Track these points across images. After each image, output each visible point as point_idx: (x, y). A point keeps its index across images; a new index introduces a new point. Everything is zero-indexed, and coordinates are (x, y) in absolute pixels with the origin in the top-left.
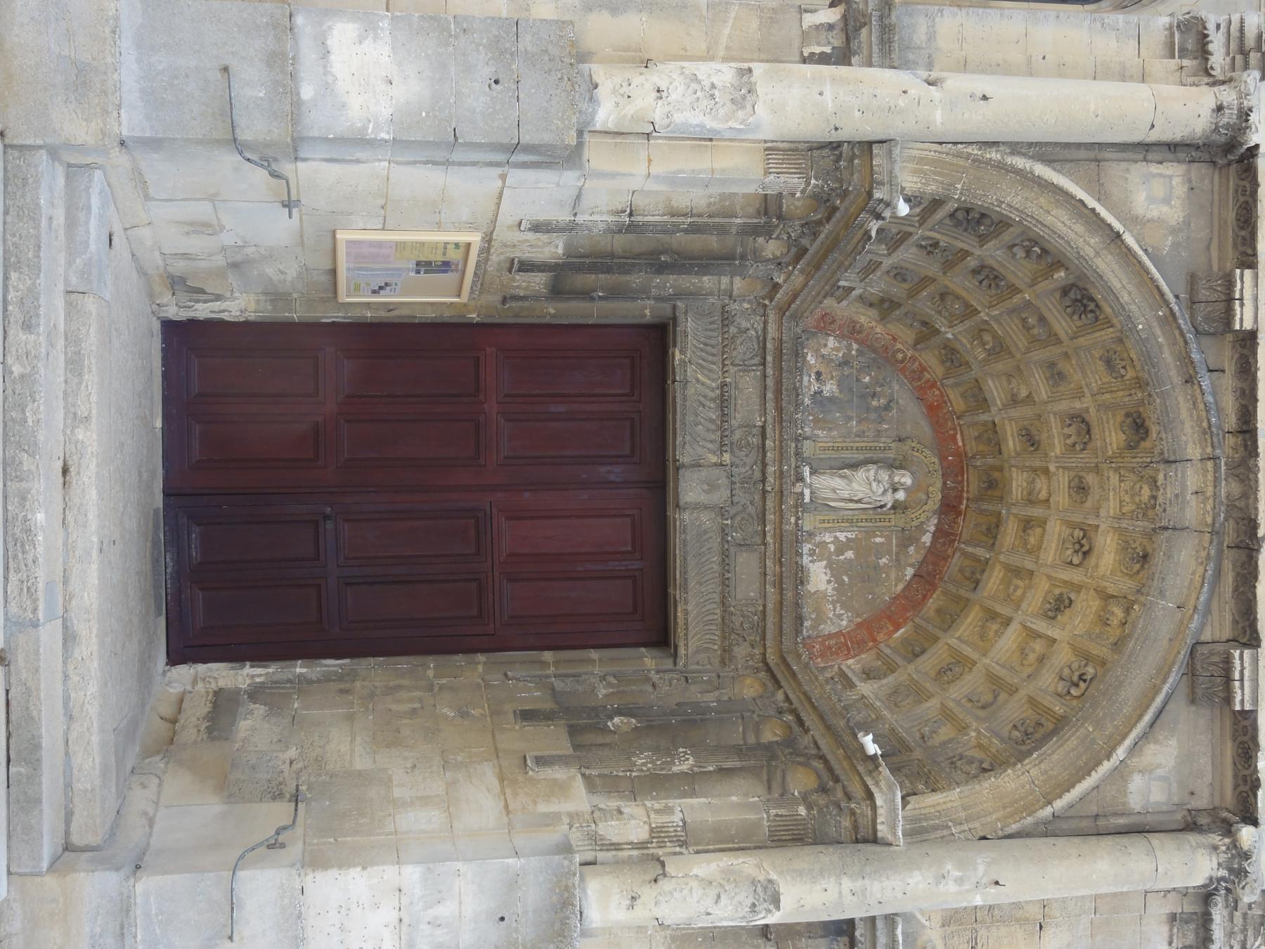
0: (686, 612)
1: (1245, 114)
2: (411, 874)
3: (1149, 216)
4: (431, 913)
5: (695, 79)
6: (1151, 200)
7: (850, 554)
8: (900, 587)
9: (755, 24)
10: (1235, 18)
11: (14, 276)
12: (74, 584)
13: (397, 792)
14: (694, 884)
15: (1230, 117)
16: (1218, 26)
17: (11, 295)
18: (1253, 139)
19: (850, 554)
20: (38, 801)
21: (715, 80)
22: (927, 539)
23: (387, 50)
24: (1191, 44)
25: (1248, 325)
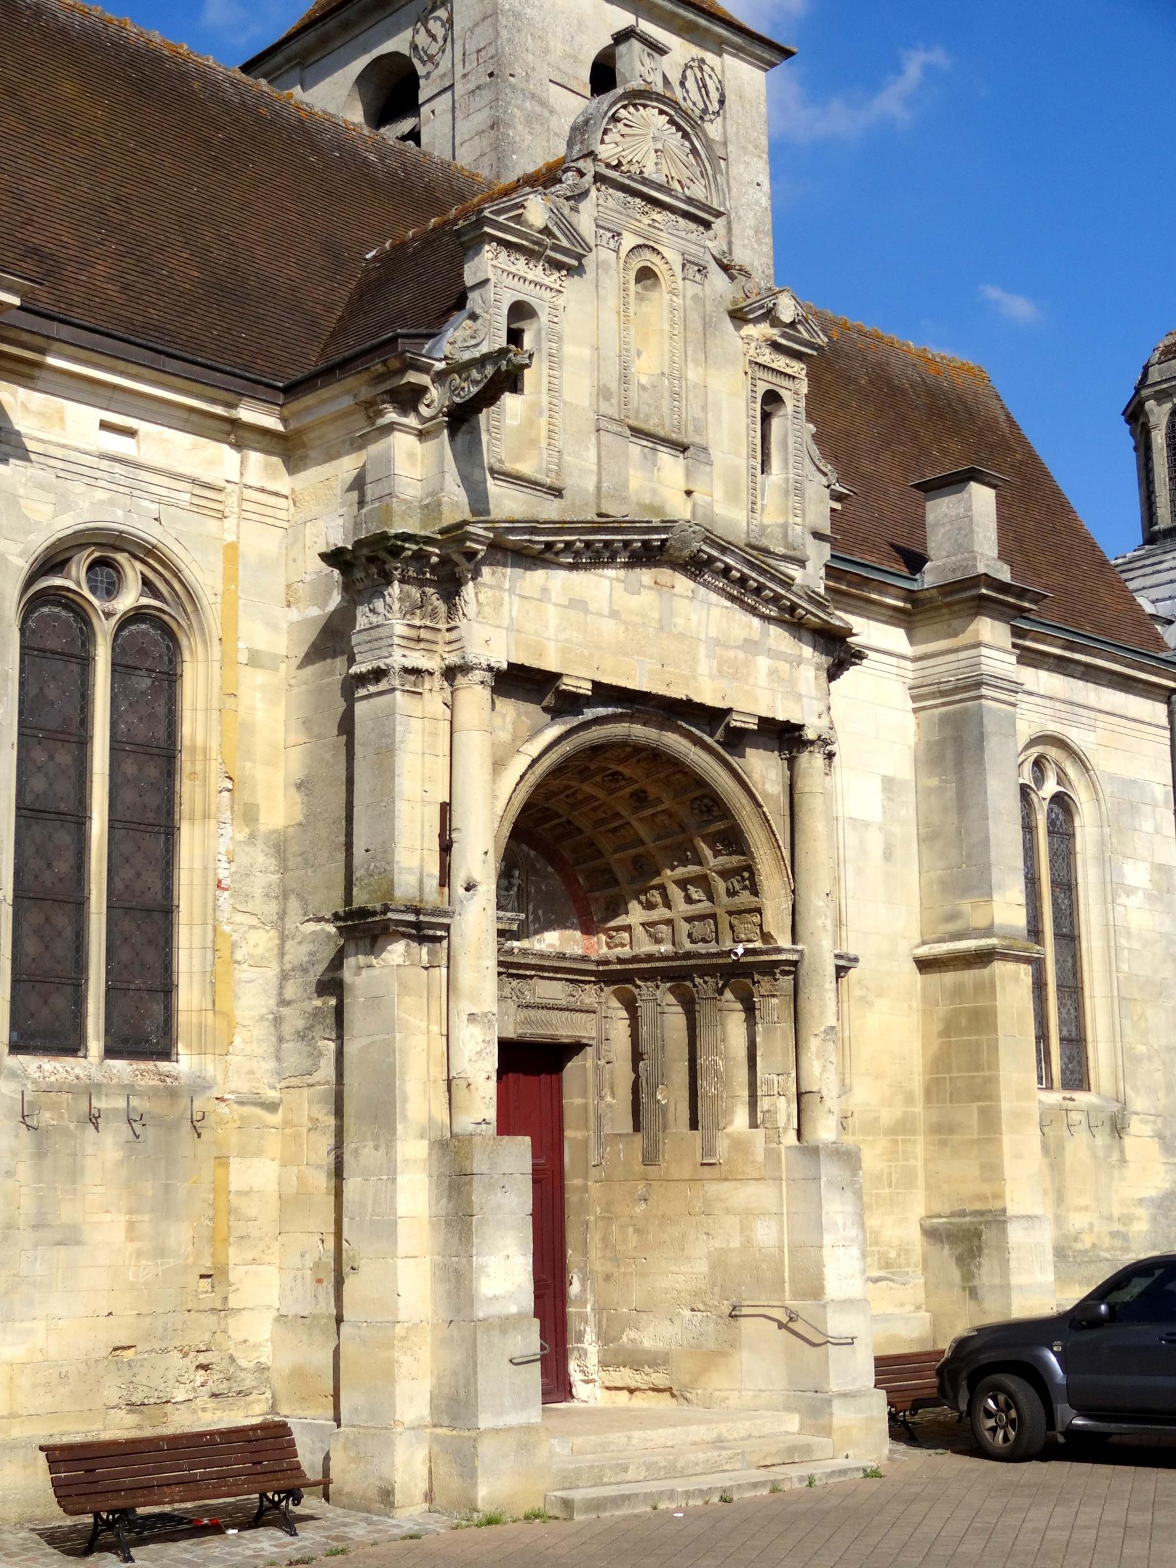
0: (567, 1037)
1: (490, 669)
2: (828, 1239)
3: (511, 731)
4: (841, 1229)
5: (479, 1053)
6: (503, 728)
7: (540, 912)
8: (557, 877)
9: (407, 999)
10: (396, 640)
11: (605, 1480)
12: (697, 1439)
13: (735, 1244)
14: (825, 1076)
15: (488, 676)
16: (404, 656)
17: (613, 1480)
18: (505, 666)
19: (540, 912)
20: (809, 1445)
21: (480, 1040)
22: (532, 853)
23: (492, 1259)
24: (412, 678)
25: (589, 686)
